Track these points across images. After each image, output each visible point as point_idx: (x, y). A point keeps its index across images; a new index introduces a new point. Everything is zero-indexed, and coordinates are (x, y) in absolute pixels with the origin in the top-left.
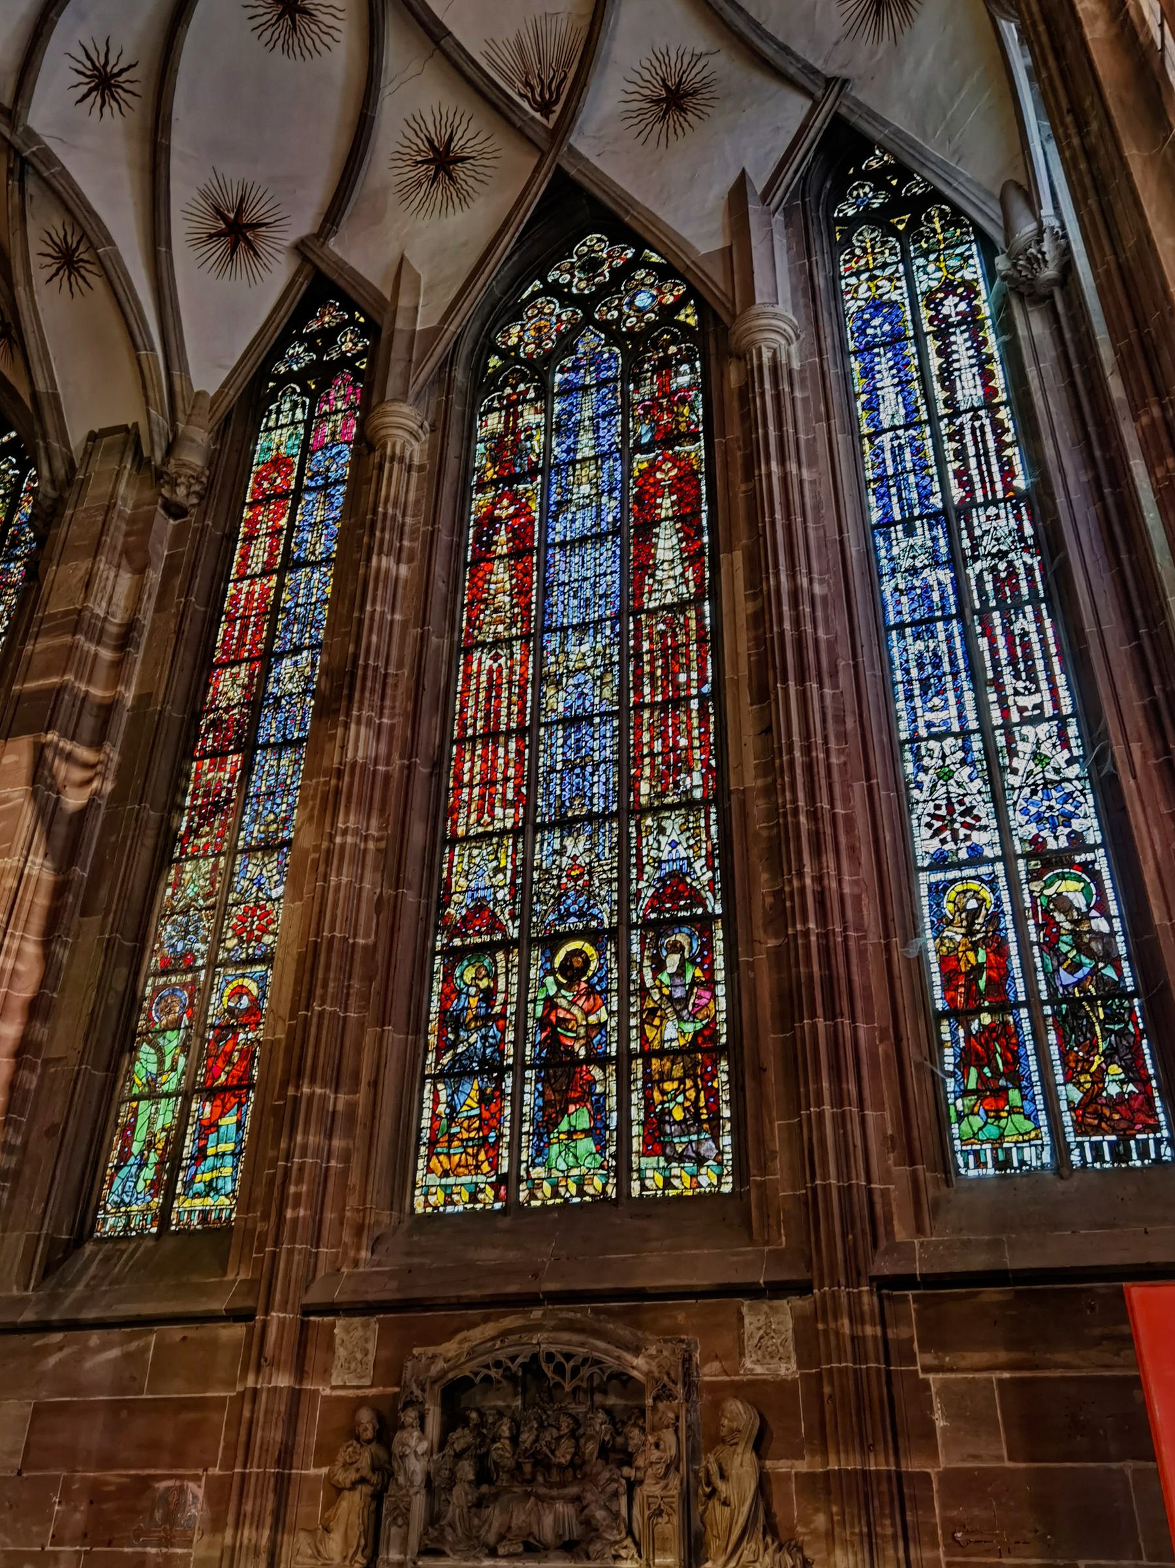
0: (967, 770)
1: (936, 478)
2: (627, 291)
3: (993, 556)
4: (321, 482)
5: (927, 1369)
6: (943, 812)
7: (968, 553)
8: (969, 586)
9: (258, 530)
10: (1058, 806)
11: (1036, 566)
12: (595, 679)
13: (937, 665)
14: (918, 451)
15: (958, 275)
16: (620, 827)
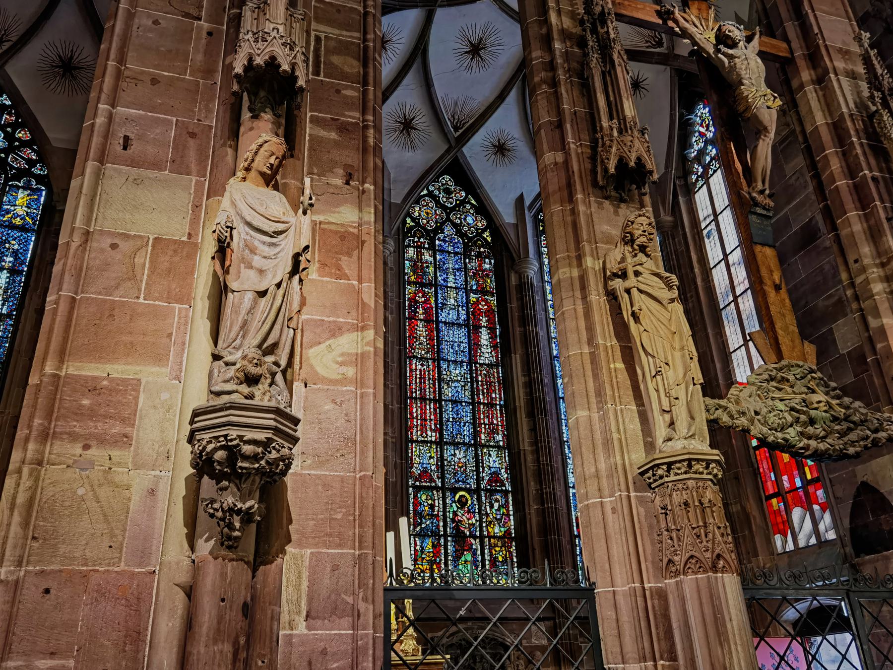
2: (464, 213)
5: (581, 643)
12: (462, 387)
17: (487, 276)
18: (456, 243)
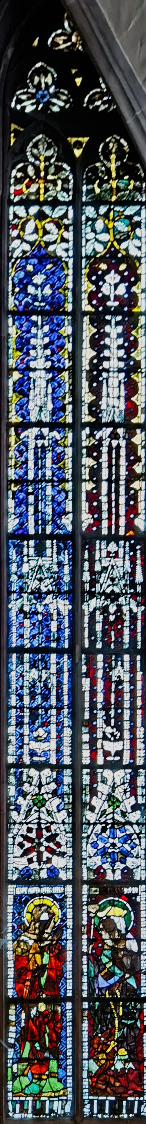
0: (57, 801)
1: (70, 495)
3: (107, 596)
6: (33, 835)
7: (87, 587)
8: (83, 623)
10: (119, 845)
11: (139, 616)
13: (46, 697)
14: (58, 458)
15: (124, 245)
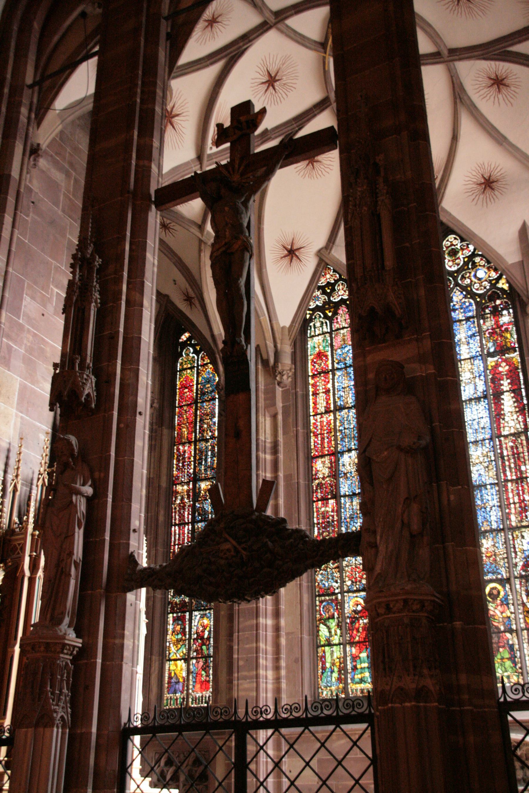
4: (343, 366)
9: (318, 390)
16: (505, 535)
17: (507, 330)
18: (467, 307)
